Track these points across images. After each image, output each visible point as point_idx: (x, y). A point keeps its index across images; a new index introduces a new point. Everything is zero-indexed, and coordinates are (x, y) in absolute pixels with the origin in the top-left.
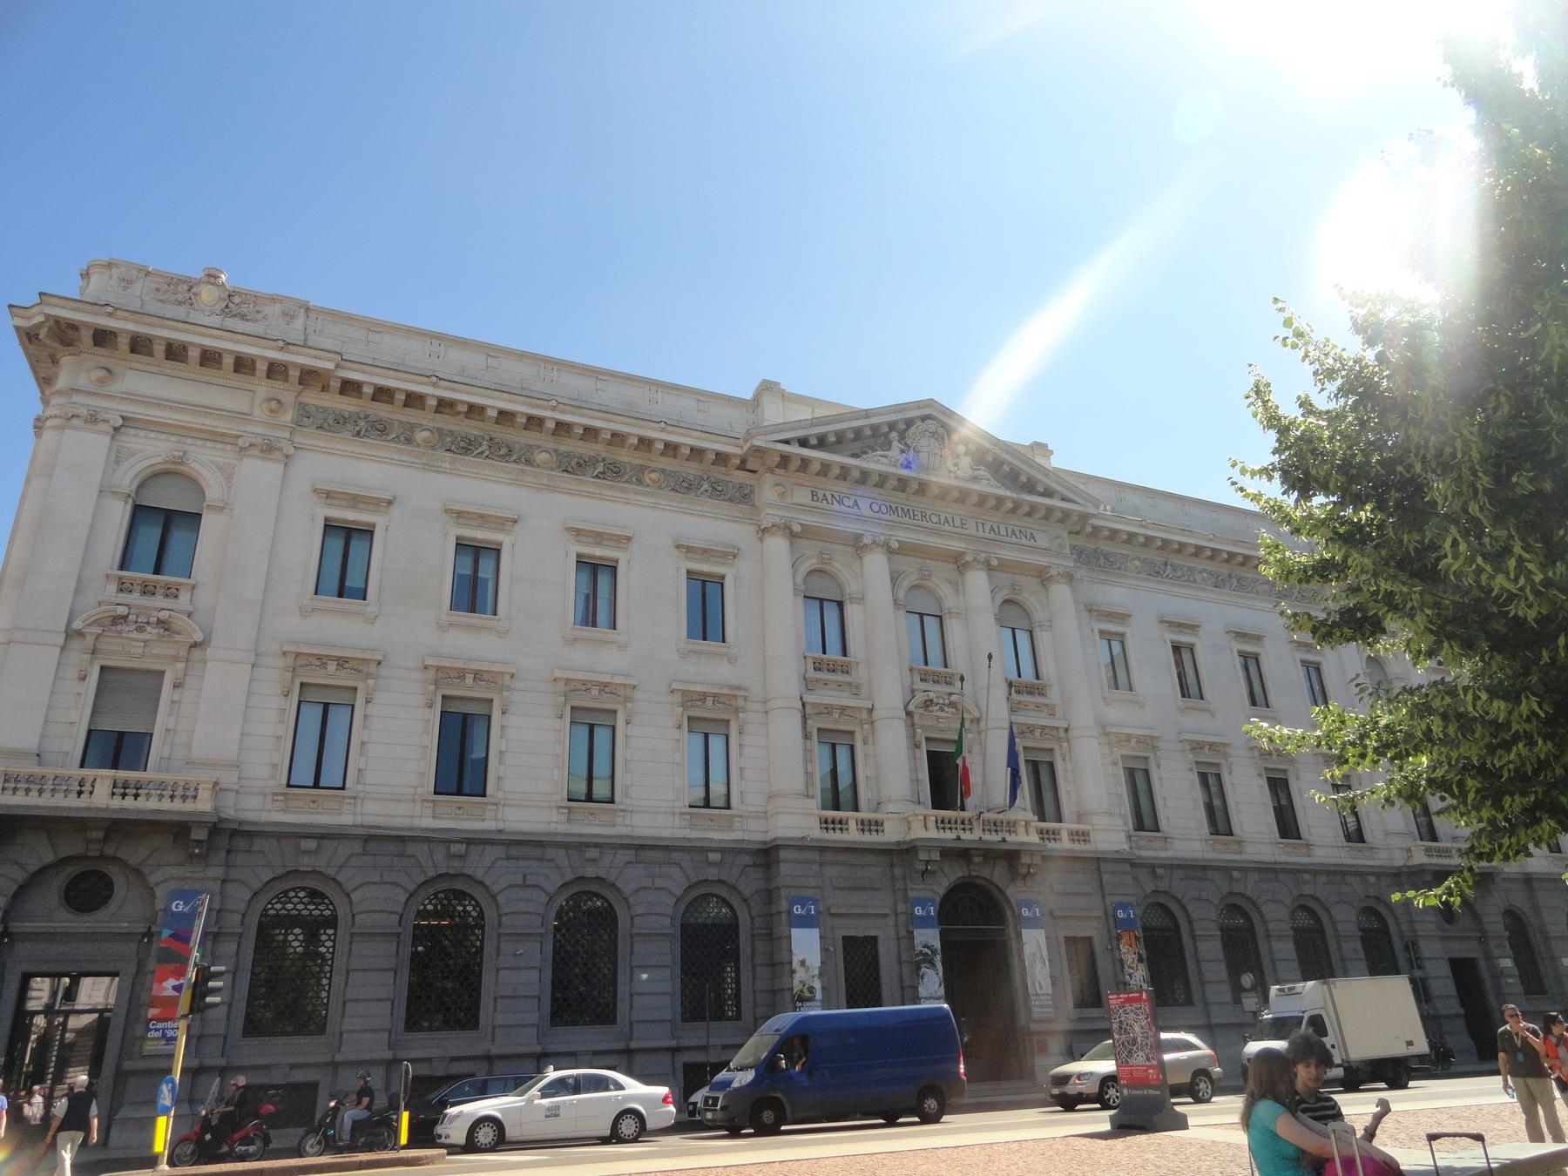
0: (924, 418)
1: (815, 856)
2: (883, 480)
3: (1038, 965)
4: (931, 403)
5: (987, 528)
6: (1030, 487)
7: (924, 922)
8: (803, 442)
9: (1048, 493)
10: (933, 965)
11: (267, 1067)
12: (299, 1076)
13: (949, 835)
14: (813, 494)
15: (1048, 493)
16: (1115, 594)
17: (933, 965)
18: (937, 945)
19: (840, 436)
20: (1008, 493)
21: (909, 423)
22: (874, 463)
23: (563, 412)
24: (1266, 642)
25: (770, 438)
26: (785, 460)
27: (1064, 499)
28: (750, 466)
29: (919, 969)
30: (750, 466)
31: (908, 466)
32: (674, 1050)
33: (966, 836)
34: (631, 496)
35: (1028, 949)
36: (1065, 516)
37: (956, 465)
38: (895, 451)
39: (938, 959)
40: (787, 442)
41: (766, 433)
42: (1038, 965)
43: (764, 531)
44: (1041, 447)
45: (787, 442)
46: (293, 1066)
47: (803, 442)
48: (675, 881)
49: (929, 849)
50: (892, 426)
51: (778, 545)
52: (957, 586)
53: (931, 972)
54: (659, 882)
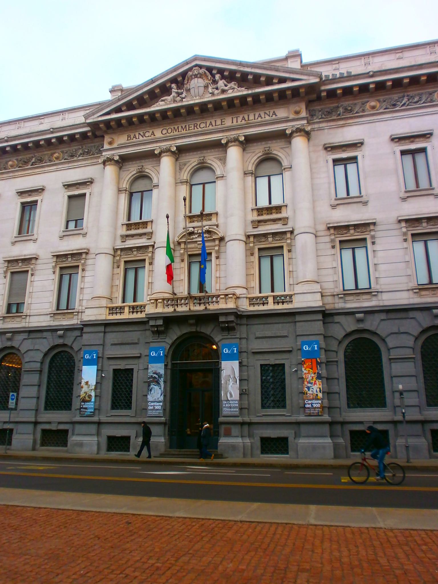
1: (102, 329)
2: (164, 113)
3: (231, 382)
4: (196, 58)
6: (269, 80)
7: (155, 360)
8: (118, 110)
9: (282, 80)
10: (158, 383)
11: (49, 423)
12: (62, 427)
13: (171, 309)
14: (129, 136)
15: (282, 80)
16: (350, 133)
17: (158, 383)
18: (162, 372)
20: (245, 92)
21: (184, 75)
23: (12, 141)
26: (107, 123)
27: (293, 80)
29: (149, 386)
32: (36, 423)
33: (180, 309)
34: (46, 169)
35: (224, 374)
36: (295, 91)
39: (162, 381)
41: (93, 114)
42: (231, 382)
43: (104, 163)
44: (296, 55)
46: (59, 423)
47: (118, 110)
48: (44, 345)
49: (156, 319)
50: (174, 80)
51: (110, 170)
52: (223, 160)
53: (156, 387)
54: (37, 347)
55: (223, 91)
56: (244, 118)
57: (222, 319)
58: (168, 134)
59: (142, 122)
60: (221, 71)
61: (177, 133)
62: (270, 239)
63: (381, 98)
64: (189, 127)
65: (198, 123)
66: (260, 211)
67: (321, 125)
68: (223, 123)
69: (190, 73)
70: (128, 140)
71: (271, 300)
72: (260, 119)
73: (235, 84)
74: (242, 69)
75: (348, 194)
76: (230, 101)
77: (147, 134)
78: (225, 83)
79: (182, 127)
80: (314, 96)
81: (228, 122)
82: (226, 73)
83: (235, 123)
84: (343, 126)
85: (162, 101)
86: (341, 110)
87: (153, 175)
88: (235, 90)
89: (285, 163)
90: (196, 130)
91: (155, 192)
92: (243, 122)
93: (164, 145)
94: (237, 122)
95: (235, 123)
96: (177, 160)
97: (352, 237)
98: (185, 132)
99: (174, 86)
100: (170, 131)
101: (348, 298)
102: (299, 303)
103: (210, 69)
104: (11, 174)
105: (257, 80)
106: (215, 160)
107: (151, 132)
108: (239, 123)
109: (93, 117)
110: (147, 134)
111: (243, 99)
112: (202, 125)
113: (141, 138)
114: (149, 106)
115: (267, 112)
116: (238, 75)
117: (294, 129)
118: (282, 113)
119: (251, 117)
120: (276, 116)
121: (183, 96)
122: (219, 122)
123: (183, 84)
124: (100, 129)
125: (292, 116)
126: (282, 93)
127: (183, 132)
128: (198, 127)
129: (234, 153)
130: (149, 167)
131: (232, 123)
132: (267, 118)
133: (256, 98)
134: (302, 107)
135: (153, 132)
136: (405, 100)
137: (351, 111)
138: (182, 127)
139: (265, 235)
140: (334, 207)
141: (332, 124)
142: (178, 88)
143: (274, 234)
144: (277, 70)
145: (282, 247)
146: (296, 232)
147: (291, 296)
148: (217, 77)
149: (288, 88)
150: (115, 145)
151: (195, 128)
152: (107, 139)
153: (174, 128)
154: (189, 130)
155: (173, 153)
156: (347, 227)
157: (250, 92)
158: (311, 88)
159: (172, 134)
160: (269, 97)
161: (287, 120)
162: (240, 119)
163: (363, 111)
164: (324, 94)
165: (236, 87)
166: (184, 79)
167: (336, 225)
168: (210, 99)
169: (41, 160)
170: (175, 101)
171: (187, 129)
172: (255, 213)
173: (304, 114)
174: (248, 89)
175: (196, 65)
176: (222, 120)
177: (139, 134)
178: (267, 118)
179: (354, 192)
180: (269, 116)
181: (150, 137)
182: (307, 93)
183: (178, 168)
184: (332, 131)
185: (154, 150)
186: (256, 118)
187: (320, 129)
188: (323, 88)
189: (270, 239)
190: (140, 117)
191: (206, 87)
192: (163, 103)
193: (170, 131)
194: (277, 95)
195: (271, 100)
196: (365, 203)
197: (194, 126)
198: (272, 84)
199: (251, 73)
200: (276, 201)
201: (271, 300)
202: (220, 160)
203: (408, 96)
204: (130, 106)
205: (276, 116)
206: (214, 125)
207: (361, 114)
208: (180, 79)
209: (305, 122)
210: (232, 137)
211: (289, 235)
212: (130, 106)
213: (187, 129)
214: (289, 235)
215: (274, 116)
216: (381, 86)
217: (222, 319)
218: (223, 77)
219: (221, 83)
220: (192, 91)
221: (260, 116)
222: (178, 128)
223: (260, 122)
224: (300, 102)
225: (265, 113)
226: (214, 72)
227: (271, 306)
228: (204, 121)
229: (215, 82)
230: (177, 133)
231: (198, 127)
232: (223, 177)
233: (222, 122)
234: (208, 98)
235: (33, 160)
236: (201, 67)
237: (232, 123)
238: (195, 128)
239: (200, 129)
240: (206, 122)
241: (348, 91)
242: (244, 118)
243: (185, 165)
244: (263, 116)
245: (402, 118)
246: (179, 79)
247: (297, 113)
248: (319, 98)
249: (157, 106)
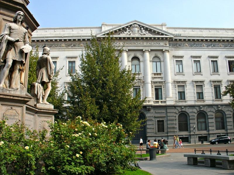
0: (134, 24)
2: (124, 38)
4: (135, 21)
5: (149, 43)
6: (158, 33)
8: (108, 34)
9: (162, 34)
15: (162, 34)
16: (180, 53)
19: (116, 31)
21: (131, 25)
22: (122, 35)
23: (65, 38)
24: (219, 58)
25: (100, 35)
26: (104, 38)
27: (166, 35)
28: (99, 40)
30: (99, 40)
31: (130, 35)
34: (78, 49)
36: (166, 38)
37: (141, 32)
38: (127, 32)
40: (104, 35)
41: (99, 34)
45: (104, 35)
50: (127, 27)
52: (143, 55)
55: (144, 34)
56: (150, 43)
57: (148, 108)
60: (143, 27)
61: (128, 45)
62: (158, 83)
63: (189, 43)
65: (135, 42)
66: (155, 74)
67: (172, 49)
71: (160, 102)
74: (150, 28)
75: (179, 72)
76: (147, 38)
77: (117, 43)
80: (171, 40)
81: (145, 44)
84: (178, 50)
86: (178, 45)
89: (162, 60)
92: (150, 45)
96: (127, 53)
97: (181, 85)
98: (130, 45)
99: (127, 28)
101: (179, 102)
102: (168, 103)
103: (139, 25)
104: (63, 49)
105: (154, 32)
107: (119, 43)
109: (99, 35)
110: (117, 43)
111: (151, 38)
112: (137, 43)
116: (149, 29)
118: (162, 44)
119: (152, 44)
121: (131, 32)
122: (142, 43)
123: (130, 28)
124: (101, 39)
125: (165, 45)
126: (162, 38)
129: (147, 54)
133: (155, 38)
136: (195, 45)
137: (181, 46)
139: (157, 82)
140: (176, 75)
141: (175, 49)
143: (159, 82)
145: (161, 86)
146: (166, 82)
147: (165, 101)
149: (164, 37)
156: (180, 82)
157: (153, 36)
158: (170, 38)
159: (126, 45)
161: (163, 46)
162: (149, 43)
163: (184, 46)
164: (174, 40)
167: (177, 81)
169: (74, 46)
172: (153, 75)
173: (168, 45)
174: (153, 35)
175: (135, 24)
178: (157, 45)
179: (181, 71)
183: (128, 56)
184: (176, 51)
187: (172, 50)
188: (174, 38)
189: (158, 83)
191: (138, 31)
192: (124, 34)
196: (184, 75)
199: (153, 30)
200: (159, 72)
201: (160, 102)
202: (141, 55)
203: (196, 44)
207: (183, 47)
208: (129, 26)
209: (169, 48)
211: (163, 83)
214: (163, 83)
216: (189, 40)
217: (148, 108)
218: (144, 29)
219: (143, 31)
220: (134, 32)
221: (155, 43)
223: (156, 46)
224: (167, 41)
227: (160, 104)
229: (141, 29)
230: (128, 45)
235: (72, 45)
241: (180, 40)
242: (150, 43)
243: (130, 55)
245: (194, 50)
246: (130, 27)
247: (166, 44)
248: (172, 40)
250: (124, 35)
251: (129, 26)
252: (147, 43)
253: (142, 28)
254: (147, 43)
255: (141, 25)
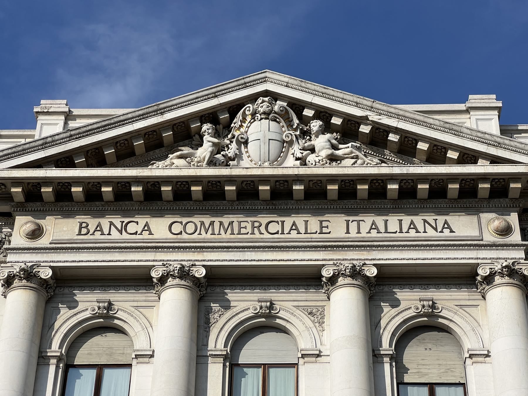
2: (182, 188)
5: (365, 227)
20: (384, 170)
43: (8, 282)
55: (333, 159)
58: (185, 236)
59: (124, 199)
61: (209, 236)
64: (240, 228)
68: (325, 230)
69: (249, 108)
70: (80, 234)
72: (412, 233)
73: (358, 149)
78: (334, 142)
79: (221, 223)
82: (336, 121)
83: (353, 233)
85: (180, 157)
87: (137, 327)
88: (359, 162)
90: (257, 235)
91: (139, 370)
92: (374, 233)
93: (177, 259)
94: (359, 232)
95: (353, 233)
98: (228, 236)
100: (190, 228)
106: (298, 312)
108: (364, 234)
110: (131, 228)
111: (377, 184)
113: (115, 235)
114: (145, 163)
115: (430, 219)
116: (365, 129)
117: (497, 267)
119: (393, 226)
120: (452, 231)
124: (9, 198)
125: (489, 237)
126: (469, 185)
127: (223, 235)
128: (263, 229)
130: (127, 305)
131: (348, 232)
132: (431, 232)
134: (514, 219)
135: (147, 225)
138: (221, 223)
142: (217, 134)
144: (457, 133)
148: (315, 125)
150: (43, 242)
151: (256, 230)
152: (23, 223)
153: (202, 223)
154: (239, 234)
155: (196, 281)
157: (397, 170)
159: (195, 236)
160: (438, 189)
162: (365, 227)
165: (361, 155)
166: (233, 116)
168: (296, 172)
170: (212, 163)
171: (236, 231)
173: (516, 237)
175: (266, 93)
176: (321, 222)
177: (111, 223)
178: (431, 232)
180: (436, 229)
181: (140, 237)
182: (524, 193)
185: (151, 268)
186: (405, 229)
190: (122, 187)
192: (182, 162)
193: (190, 228)
194: (457, 186)
195: (439, 196)
197: (253, 227)
198: (443, 160)
199: (397, 131)
204: (95, 156)
205: (452, 231)
206: (302, 230)
210: (347, 264)
212: (95, 156)
213: (236, 231)
215: (447, 232)
222: (212, 223)
225: (425, 221)
226: (308, 113)
228: (280, 219)
229: (305, 134)
231: (263, 229)
232: (318, 356)
233: (322, 227)
234: (290, 166)
236: (275, 97)
237: (348, 232)
238: (256, 230)
239: (267, 236)
240: (283, 222)
242: (374, 226)
244: (421, 228)
249: (165, 167)
250: (185, 167)
251: (224, 116)
252: (353, 227)
253: (315, 125)
254: (353, 227)
255: (311, 105)
